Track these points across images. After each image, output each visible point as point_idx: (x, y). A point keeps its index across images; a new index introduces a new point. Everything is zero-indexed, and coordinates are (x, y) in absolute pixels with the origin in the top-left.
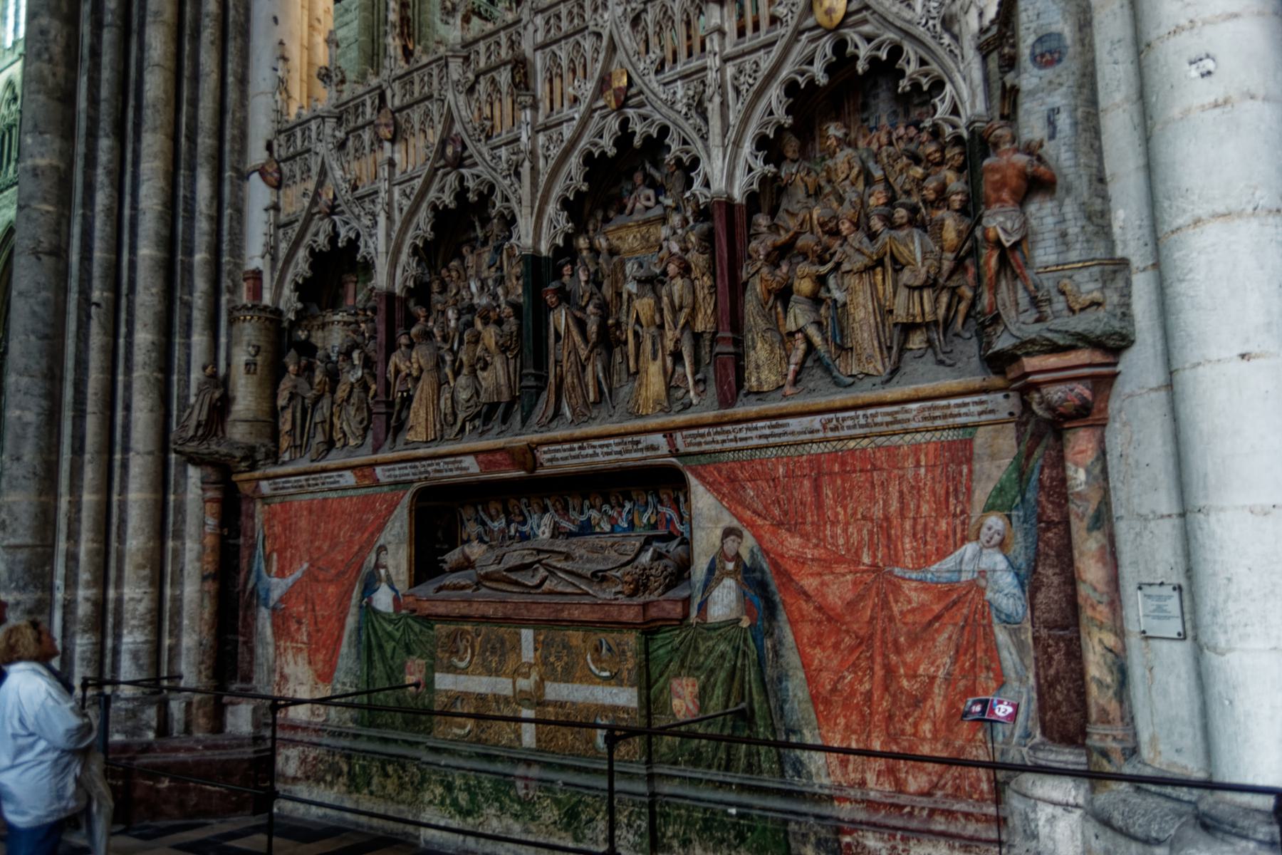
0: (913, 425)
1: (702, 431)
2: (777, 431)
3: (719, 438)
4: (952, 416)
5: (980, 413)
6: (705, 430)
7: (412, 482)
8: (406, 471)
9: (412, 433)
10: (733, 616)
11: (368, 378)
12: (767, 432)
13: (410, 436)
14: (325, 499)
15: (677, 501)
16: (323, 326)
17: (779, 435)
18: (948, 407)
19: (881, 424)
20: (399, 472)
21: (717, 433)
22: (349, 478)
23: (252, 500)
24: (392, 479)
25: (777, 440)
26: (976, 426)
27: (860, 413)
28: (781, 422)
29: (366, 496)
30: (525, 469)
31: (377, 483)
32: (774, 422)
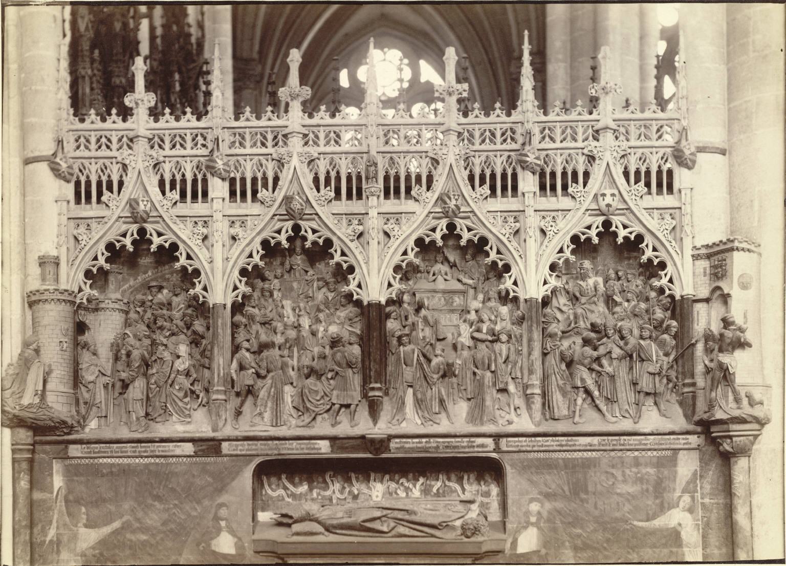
0: (649, 447)
1: (521, 439)
2: (570, 443)
3: (531, 444)
4: (670, 444)
5: (684, 444)
6: (524, 439)
7: (258, 456)
10: (535, 549)
12: (564, 443)
15: (462, 478)
17: (570, 446)
18: (669, 439)
19: (631, 445)
21: (531, 441)
25: (568, 448)
26: (680, 449)
27: (622, 438)
28: (574, 438)
30: (371, 453)
32: (570, 438)
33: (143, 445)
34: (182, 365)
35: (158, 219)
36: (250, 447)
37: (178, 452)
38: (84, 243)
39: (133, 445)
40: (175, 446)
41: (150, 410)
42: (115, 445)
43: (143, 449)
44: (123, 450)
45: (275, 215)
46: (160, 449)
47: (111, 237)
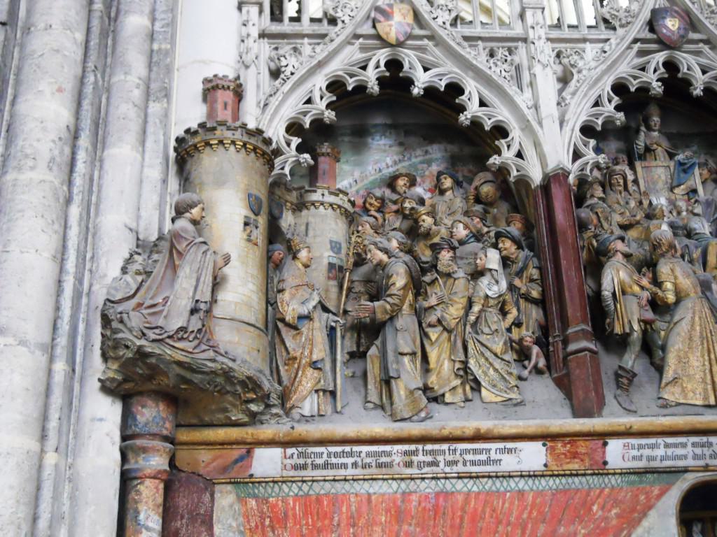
7: (685, 470)
8: (680, 451)
9: (677, 390)
11: (508, 297)
13: (671, 394)
14: (447, 495)
16: (300, 206)
20: (660, 452)
22: (533, 456)
23: (210, 484)
24: (641, 464)
29: (565, 492)
31: (601, 469)
33: (429, 447)
34: (492, 287)
35: (426, 42)
36: (670, 451)
37: (508, 463)
38: (290, 69)
39: (406, 447)
40: (502, 451)
41: (433, 380)
42: (365, 449)
43: (429, 459)
44: (383, 459)
45: (635, 41)
46: (469, 457)
47: (336, 67)
